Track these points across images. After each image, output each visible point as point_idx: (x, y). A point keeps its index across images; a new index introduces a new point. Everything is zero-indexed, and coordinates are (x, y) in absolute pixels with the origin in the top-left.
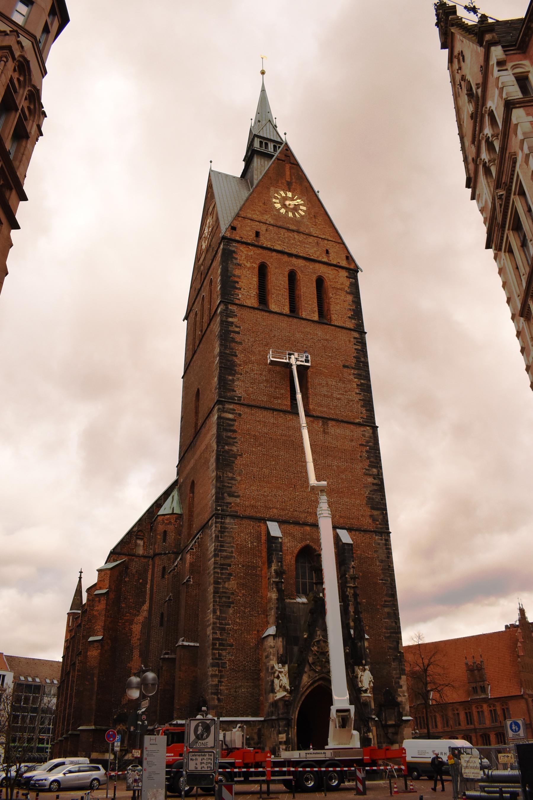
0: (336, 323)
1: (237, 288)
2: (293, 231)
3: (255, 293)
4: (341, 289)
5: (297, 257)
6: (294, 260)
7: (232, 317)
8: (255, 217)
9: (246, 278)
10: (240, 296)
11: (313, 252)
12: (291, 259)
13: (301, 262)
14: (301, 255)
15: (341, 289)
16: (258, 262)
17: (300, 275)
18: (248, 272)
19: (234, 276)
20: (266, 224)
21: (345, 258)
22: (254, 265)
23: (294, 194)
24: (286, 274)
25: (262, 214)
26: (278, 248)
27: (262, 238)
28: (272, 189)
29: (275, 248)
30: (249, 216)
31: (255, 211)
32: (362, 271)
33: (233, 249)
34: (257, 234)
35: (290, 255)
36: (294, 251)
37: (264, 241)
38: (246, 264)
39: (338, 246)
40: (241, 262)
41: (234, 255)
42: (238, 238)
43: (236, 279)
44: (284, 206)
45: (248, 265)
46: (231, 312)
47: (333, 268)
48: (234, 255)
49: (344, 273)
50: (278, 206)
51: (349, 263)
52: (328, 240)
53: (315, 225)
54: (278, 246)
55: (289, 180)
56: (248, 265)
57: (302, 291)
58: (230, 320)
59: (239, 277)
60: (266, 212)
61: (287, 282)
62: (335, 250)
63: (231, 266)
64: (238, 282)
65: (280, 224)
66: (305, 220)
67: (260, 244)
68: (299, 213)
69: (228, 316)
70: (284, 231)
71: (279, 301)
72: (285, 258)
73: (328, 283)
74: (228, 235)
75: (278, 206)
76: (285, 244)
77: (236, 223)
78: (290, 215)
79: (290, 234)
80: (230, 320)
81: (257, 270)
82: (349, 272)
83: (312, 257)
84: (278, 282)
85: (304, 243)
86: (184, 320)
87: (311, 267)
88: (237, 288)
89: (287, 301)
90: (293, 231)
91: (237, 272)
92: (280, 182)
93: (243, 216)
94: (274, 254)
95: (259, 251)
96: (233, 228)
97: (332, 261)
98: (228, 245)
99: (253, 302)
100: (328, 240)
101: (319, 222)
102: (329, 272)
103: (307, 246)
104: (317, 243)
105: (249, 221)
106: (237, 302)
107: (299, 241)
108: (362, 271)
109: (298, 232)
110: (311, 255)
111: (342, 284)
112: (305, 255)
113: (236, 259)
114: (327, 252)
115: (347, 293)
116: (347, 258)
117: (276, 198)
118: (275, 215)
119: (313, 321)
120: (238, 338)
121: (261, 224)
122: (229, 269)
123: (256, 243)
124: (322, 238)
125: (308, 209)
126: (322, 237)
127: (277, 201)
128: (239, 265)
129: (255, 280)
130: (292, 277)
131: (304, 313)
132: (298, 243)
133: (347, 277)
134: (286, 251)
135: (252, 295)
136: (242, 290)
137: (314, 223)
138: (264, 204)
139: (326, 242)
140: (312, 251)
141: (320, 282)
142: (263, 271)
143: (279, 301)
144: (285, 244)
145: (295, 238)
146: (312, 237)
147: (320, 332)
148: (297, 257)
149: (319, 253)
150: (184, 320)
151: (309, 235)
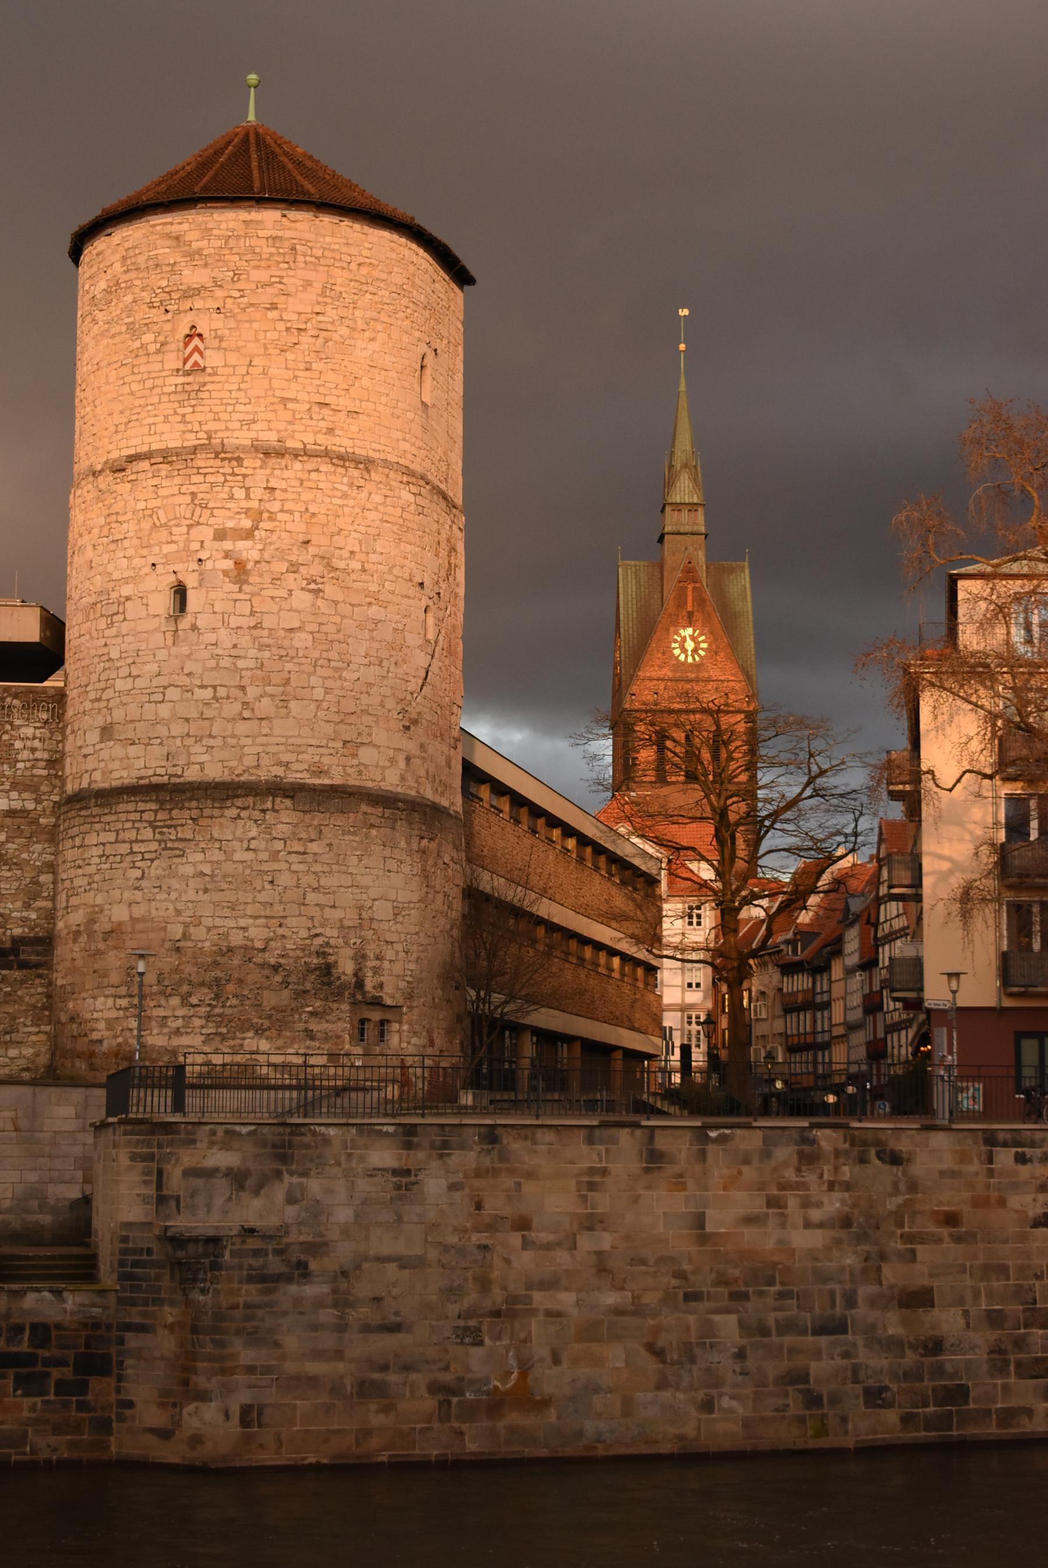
2: (691, 681)
8: (653, 674)
25: (660, 667)
28: (672, 629)
31: (653, 666)
44: (684, 650)
50: (677, 652)
65: (678, 675)
68: (699, 655)
78: (690, 660)
79: (689, 686)
90: (691, 681)
105: (648, 682)
117: (676, 641)
127: (677, 645)
138: (663, 653)
139: (726, 684)
151: (709, 680)
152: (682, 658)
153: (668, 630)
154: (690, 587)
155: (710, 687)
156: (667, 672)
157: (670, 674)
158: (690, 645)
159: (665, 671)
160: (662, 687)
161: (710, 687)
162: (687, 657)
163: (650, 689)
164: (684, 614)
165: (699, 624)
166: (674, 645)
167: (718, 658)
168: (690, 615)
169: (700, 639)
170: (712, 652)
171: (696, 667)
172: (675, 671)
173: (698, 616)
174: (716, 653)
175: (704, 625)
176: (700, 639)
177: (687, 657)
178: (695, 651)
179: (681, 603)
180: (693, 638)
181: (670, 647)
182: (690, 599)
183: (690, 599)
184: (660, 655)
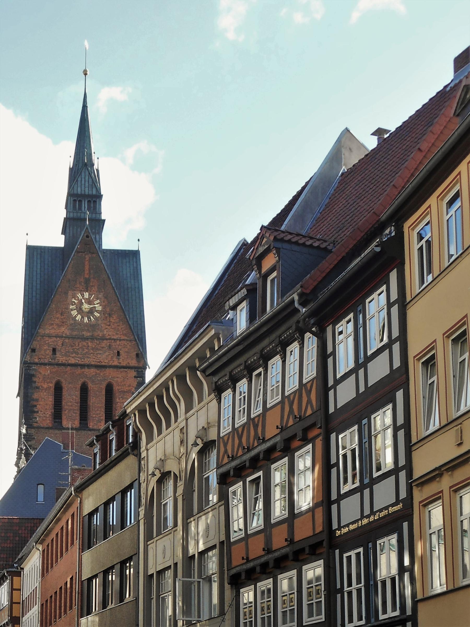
1: (35, 412)
2: (87, 339)
3: (50, 413)
5: (89, 366)
6: (86, 370)
7: (31, 441)
8: (52, 331)
9: (43, 400)
10: (38, 419)
11: (105, 357)
12: (83, 370)
13: (93, 370)
14: (93, 363)
16: (54, 382)
17: (90, 385)
18: (45, 394)
19: (33, 400)
20: (62, 337)
21: (135, 357)
22: (51, 385)
23: (91, 293)
24: (79, 386)
25: (59, 326)
26: (72, 361)
27: (58, 354)
28: (70, 293)
29: (70, 362)
30: (47, 332)
31: (52, 324)
32: (149, 368)
33: (32, 373)
34: (54, 350)
35: (83, 366)
36: (86, 361)
37: (60, 358)
38: (44, 386)
39: (130, 344)
40: (39, 384)
41: (34, 379)
42: (36, 360)
43: (35, 403)
46: (29, 436)
47: (123, 370)
48: (34, 379)
49: (133, 373)
50: (74, 313)
51: (139, 362)
52: (120, 340)
53: (109, 326)
54: (73, 359)
55: (87, 277)
56: (45, 386)
57: (91, 402)
59: (37, 400)
60: (63, 323)
61: (79, 396)
62: (126, 350)
64: (36, 406)
65: (75, 333)
66: (100, 322)
70: (79, 340)
72: (79, 371)
73: (116, 388)
74: (28, 359)
75: (74, 313)
76: (79, 356)
78: (86, 320)
79: (85, 344)
81: (52, 390)
82: (137, 371)
83: (103, 364)
84: (71, 398)
85: (97, 349)
86: (17, 397)
87: (102, 374)
88: (35, 412)
89: (78, 415)
90: (87, 339)
91: (36, 396)
92: (78, 282)
93: (41, 334)
94: (69, 368)
95: (56, 369)
96: (33, 350)
97: (122, 363)
98: (28, 369)
99: (48, 422)
100: (120, 340)
101: (113, 321)
102: (118, 376)
103: (101, 352)
104: (110, 346)
105: (47, 338)
106: (35, 425)
107: (93, 349)
108: (149, 368)
109: (92, 338)
110: (102, 361)
111: (129, 386)
112: (96, 363)
113: (35, 382)
114: (118, 353)
116: (137, 355)
118: (71, 325)
121: (58, 339)
122: (29, 395)
123: (53, 361)
124: (114, 340)
125: (104, 307)
126: (115, 338)
128: (37, 388)
129: (50, 400)
131: (91, 424)
132: (92, 351)
133: (135, 377)
134: (80, 362)
135: (47, 416)
136: (39, 412)
137: (108, 324)
138: (62, 314)
139: (118, 342)
140: (104, 356)
144: (79, 356)
145: (88, 346)
146: (105, 341)
148: (89, 366)
149: (110, 356)
150: (17, 397)
151: (103, 338)
153: (66, 293)
154: (87, 257)
155: (103, 345)
156: (64, 330)
157: (68, 333)
158: (86, 307)
159: (63, 329)
160: (60, 343)
161: (103, 345)
164: (82, 280)
166: (71, 307)
167: (111, 319)
168: (87, 281)
170: (107, 314)
172: (72, 330)
174: (110, 315)
177: (83, 317)
178: (91, 311)
181: (67, 308)
182: (87, 267)
183: (87, 267)
184: (59, 315)
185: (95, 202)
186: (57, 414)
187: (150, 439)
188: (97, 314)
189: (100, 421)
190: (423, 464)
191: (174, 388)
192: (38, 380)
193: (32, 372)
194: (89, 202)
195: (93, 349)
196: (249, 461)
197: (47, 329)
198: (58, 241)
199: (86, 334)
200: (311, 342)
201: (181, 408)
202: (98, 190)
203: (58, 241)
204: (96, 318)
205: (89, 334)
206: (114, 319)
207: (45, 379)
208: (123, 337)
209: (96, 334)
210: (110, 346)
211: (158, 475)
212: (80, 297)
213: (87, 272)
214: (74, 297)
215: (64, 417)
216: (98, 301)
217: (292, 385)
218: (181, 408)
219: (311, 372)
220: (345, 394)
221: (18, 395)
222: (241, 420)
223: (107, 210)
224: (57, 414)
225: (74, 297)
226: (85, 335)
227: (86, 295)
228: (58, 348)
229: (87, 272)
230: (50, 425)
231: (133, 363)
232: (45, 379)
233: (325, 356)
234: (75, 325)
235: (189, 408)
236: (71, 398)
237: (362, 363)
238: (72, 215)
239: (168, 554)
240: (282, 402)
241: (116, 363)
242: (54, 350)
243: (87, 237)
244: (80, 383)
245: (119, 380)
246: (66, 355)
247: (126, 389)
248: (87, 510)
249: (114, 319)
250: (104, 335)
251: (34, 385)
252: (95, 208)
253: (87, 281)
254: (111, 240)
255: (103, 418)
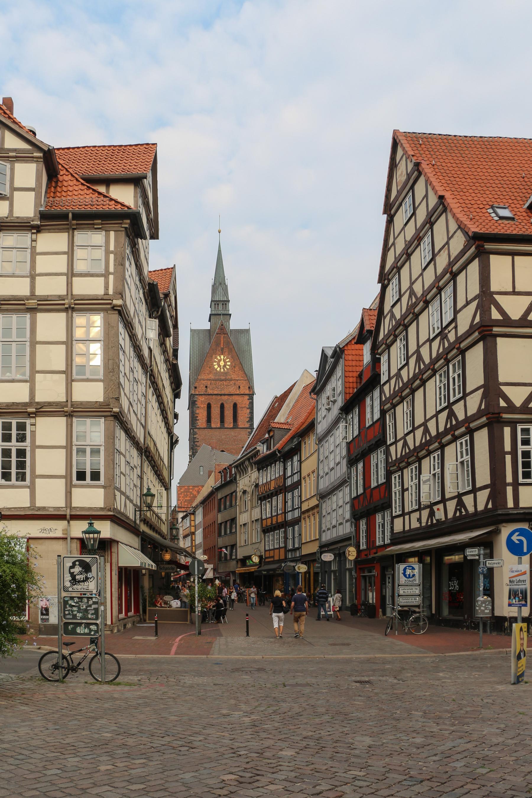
0: (241, 427)
4: (244, 407)
5: (224, 395)
6: (223, 397)
8: (205, 377)
11: (232, 390)
13: (226, 397)
15: (244, 407)
17: (225, 405)
19: (196, 414)
24: (219, 406)
25: (208, 374)
26: (216, 392)
28: (214, 356)
30: (202, 377)
34: (206, 387)
35: (221, 395)
36: (223, 392)
37: (210, 391)
42: (197, 393)
44: (219, 366)
45: (202, 406)
48: (196, 403)
49: (247, 397)
50: (216, 367)
51: (250, 391)
56: (202, 406)
58: (195, 436)
59: (198, 414)
63: (195, 409)
65: (217, 377)
67: (207, 393)
68: (226, 368)
69: (194, 435)
71: (216, 422)
72: (219, 397)
74: (193, 392)
75: (216, 367)
77: (196, 385)
78: (222, 370)
80: (195, 436)
81: (206, 408)
84: (216, 411)
91: (197, 412)
94: (214, 396)
95: (207, 397)
96: (196, 388)
99: (204, 425)
104: (235, 384)
106: (198, 427)
107: (226, 385)
114: (239, 387)
115: (247, 408)
116: (249, 387)
117: (215, 362)
119: (230, 428)
120: (198, 444)
123: (206, 393)
125: (231, 363)
127: (216, 364)
128: (198, 407)
129: (205, 413)
130: (222, 406)
138: (209, 368)
140: (232, 389)
141: (235, 406)
142: (209, 406)
143: (216, 422)
147: (233, 433)
148: (224, 395)
152: (218, 369)
153: (212, 356)
155: (231, 383)
156: (211, 376)
157: (213, 377)
158: (222, 363)
160: (209, 383)
161: (231, 383)
162: (220, 369)
163: (203, 384)
164: (220, 349)
165: (227, 353)
166: (214, 364)
168: (222, 349)
169: (227, 360)
170: (233, 367)
171: (225, 374)
173: (226, 350)
174: (234, 367)
175: (229, 354)
176: (227, 360)
177: (220, 369)
178: (225, 366)
179: (218, 344)
180: (224, 360)
182: (222, 341)
183: (222, 341)
185: (226, 304)
186: (209, 420)
187: (240, 477)
188: (228, 367)
189: (230, 423)
190: (305, 507)
191: (247, 463)
192: (199, 404)
193: (195, 399)
194: (223, 304)
195: (226, 385)
196: (265, 496)
197: (202, 377)
198: (207, 326)
199: (223, 378)
200: (282, 464)
201: (249, 469)
202: (228, 297)
203: (207, 326)
204: (227, 369)
205: (224, 378)
206: (237, 369)
207: (202, 402)
208: (242, 379)
209: (227, 377)
210: (235, 384)
211: (242, 491)
212: (219, 358)
213: (222, 344)
214: (216, 358)
215: (212, 422)
216: (228, 360)
217: (277, 475)
218: (249, 469)
219: (281, 473)
220: (289, 482)
221: (188, 409)
222: (265, 481)
223: (232, 308)
224: (209, 420)
225: (216, 358)
226: (222, 378)
227: (222, 357)
228: (208, 386)
229: (222, 344)
230: (205, 427)
231: (247, 392)
232: (202, 402)
233: (285, 469)
234: (217, 373)
235: (252, 470)
236: (216, 411)
237: (293, 475)
238: (213, 312)
239: (246, 519)
240: (275, 479)
241: (238, 393)
242: (206, 387)
243: (222, 325)
244: (220, 404)
245: (240, 401)
246: (212, 389)
247: (243, 406)
248: (219, 497)
249: (237, 369)
250: (232, 378)
251: (196, 406)
252: (226, 308)
253: (222, 349)
254: (234, 324)
255: (232, 421)
